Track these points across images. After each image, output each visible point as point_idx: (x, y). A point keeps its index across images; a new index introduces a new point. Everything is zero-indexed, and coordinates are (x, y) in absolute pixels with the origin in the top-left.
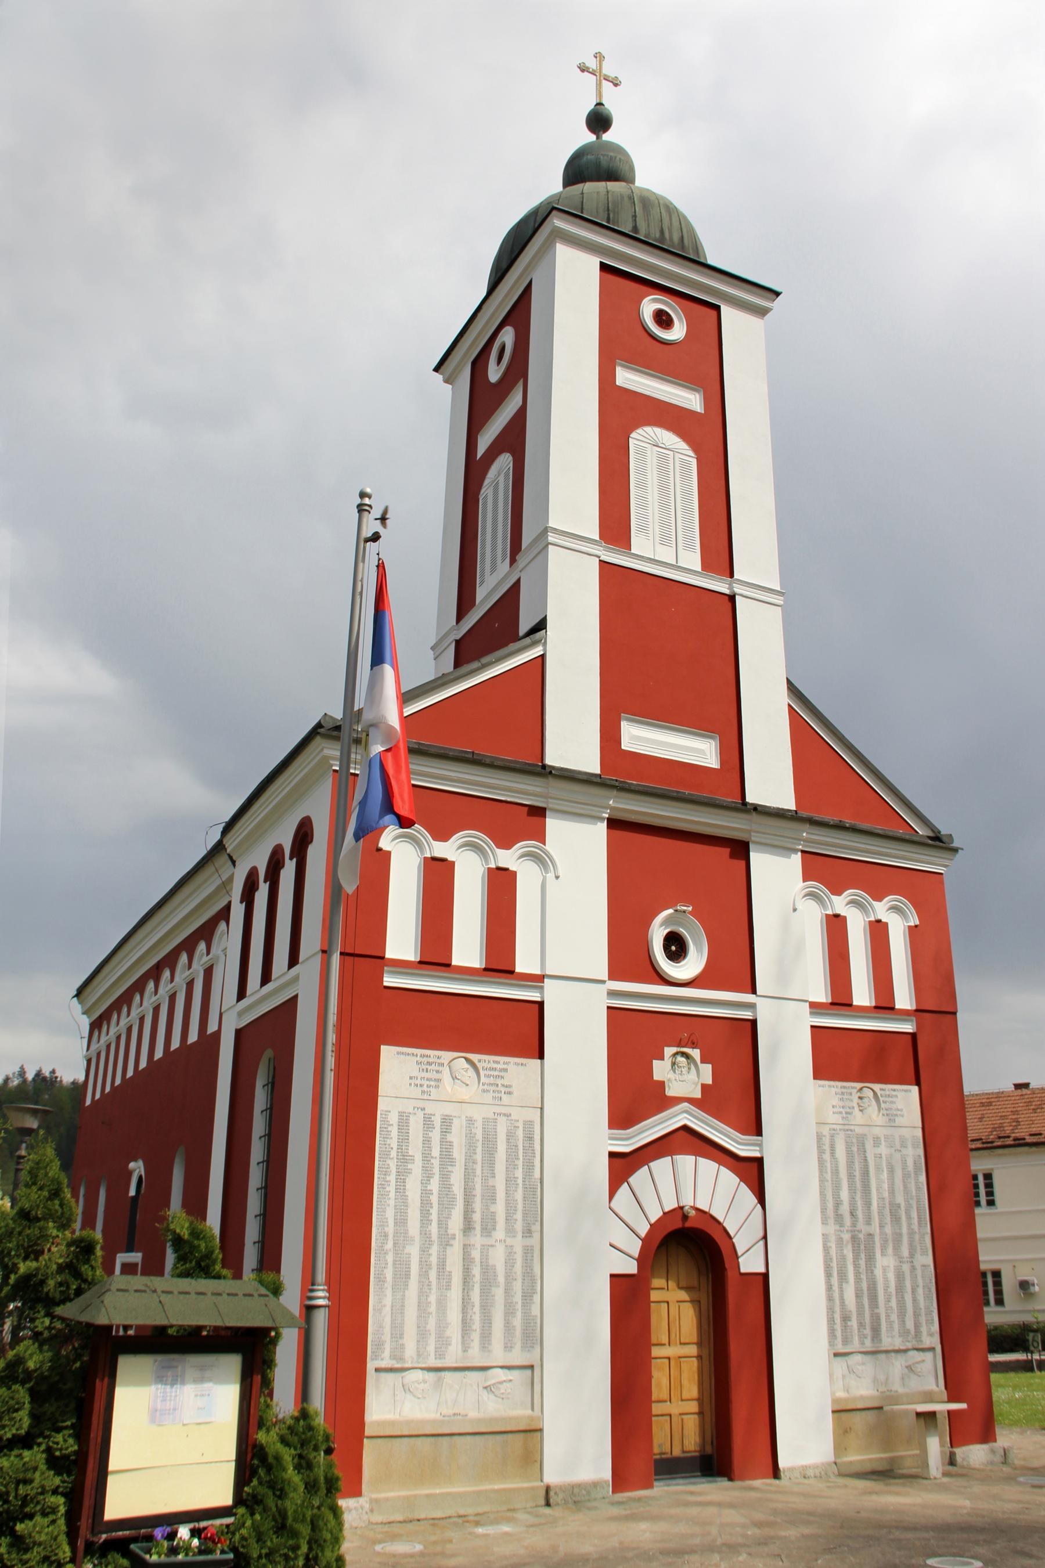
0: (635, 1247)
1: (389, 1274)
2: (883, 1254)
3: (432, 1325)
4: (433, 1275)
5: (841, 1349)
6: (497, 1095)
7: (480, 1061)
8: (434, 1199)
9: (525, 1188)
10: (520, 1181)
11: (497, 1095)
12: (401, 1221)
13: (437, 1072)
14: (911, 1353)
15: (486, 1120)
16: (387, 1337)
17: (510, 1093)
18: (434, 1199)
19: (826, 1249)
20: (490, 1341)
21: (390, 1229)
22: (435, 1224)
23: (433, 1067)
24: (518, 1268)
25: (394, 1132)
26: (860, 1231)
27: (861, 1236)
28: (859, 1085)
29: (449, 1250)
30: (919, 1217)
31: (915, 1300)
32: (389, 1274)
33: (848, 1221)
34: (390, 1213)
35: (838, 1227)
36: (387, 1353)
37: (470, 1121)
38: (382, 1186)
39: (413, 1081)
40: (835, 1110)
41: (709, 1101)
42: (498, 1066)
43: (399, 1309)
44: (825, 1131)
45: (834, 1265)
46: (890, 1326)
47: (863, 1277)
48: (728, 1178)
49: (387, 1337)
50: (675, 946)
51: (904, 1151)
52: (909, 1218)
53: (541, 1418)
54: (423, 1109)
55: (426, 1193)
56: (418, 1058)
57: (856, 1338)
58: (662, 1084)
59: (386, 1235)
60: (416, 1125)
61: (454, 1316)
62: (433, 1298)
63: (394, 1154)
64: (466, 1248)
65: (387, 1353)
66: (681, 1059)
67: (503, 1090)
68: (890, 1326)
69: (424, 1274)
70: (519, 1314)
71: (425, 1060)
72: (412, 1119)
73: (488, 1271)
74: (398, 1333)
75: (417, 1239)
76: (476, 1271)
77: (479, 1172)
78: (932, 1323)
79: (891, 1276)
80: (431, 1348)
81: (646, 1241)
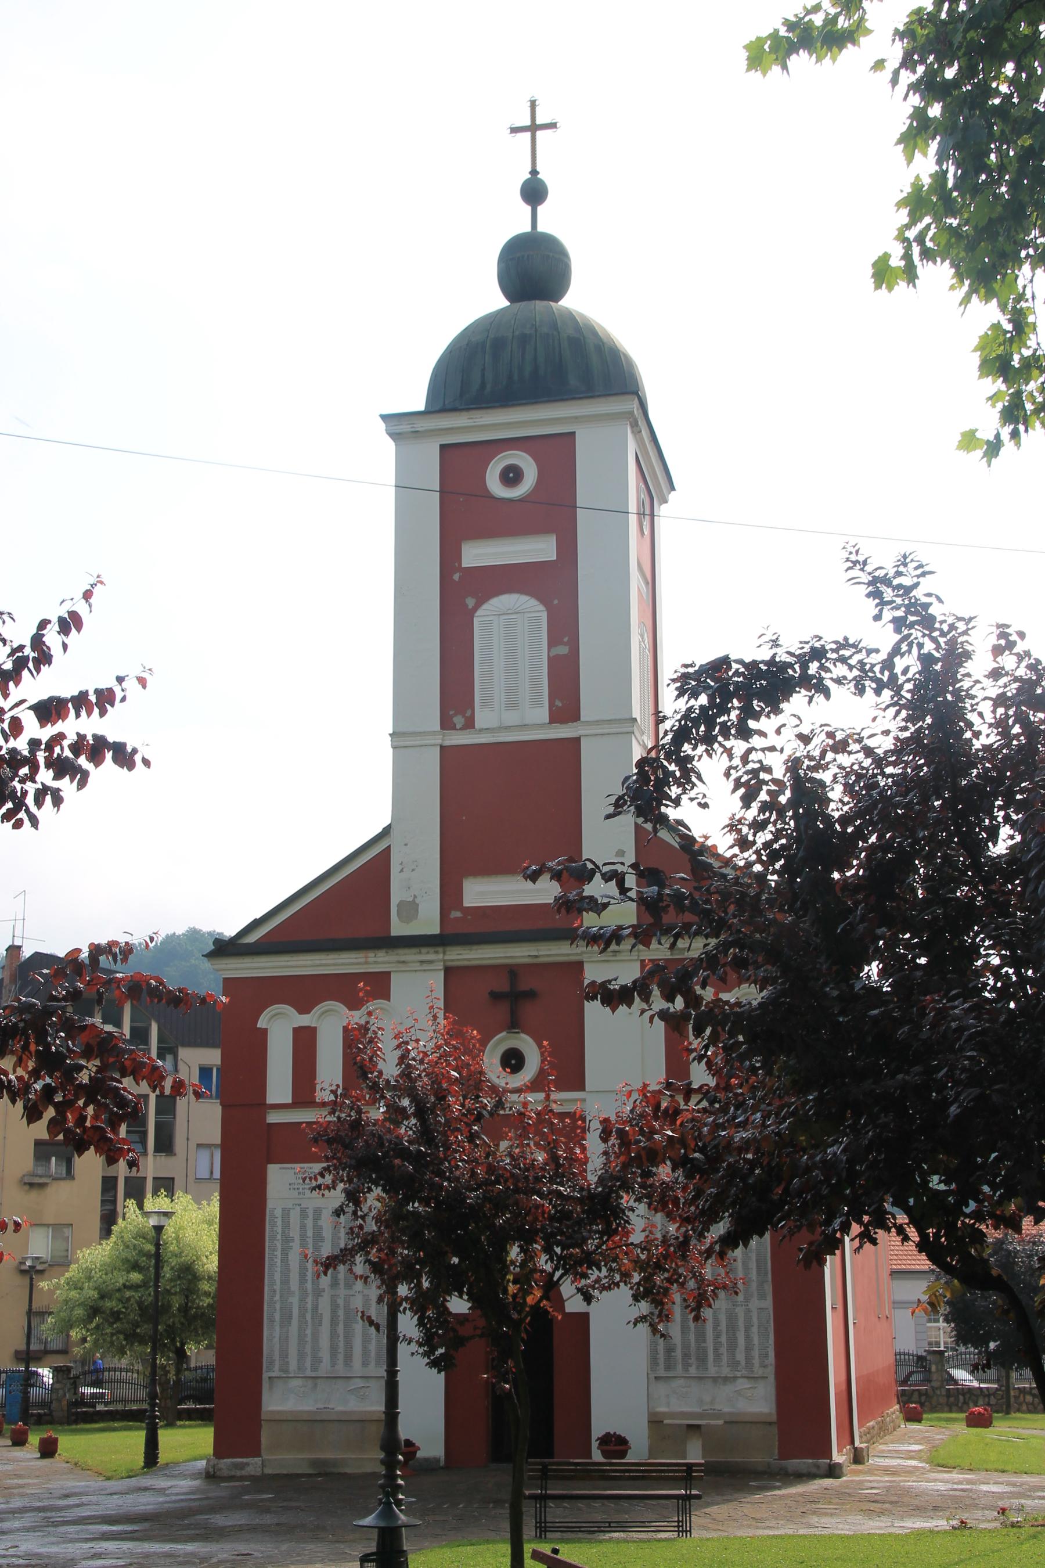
1: (277, 1316)
3: (308, 1349)
4: (309, 1316)
5: (662, 1373)
12: (285, 1281)
14: (740, 1380)
16: (276, 1357)
20: (351, 1360)
21: (277, 1287)
25: (279, 1223)
30: (758, 1267)
31: (748, 1338)
32: (277, 1316)
34: (277, 1277)
36: (277, 1367)
38: (271, 1259)
43: (285, 1340)
46: (718, 1356)
49: (276, 1357)
57: (680, 1367)
59: (275, 1291)
62: (309, 1332)
63: (279, 1237)
65: (277, 1367)
68: (718, 1356)
70: (374, 1342)
74: (284, 1355)
75: (297, 1293)
76: (341, 1313)
78: (767, 1356)
80: (308, 1364)
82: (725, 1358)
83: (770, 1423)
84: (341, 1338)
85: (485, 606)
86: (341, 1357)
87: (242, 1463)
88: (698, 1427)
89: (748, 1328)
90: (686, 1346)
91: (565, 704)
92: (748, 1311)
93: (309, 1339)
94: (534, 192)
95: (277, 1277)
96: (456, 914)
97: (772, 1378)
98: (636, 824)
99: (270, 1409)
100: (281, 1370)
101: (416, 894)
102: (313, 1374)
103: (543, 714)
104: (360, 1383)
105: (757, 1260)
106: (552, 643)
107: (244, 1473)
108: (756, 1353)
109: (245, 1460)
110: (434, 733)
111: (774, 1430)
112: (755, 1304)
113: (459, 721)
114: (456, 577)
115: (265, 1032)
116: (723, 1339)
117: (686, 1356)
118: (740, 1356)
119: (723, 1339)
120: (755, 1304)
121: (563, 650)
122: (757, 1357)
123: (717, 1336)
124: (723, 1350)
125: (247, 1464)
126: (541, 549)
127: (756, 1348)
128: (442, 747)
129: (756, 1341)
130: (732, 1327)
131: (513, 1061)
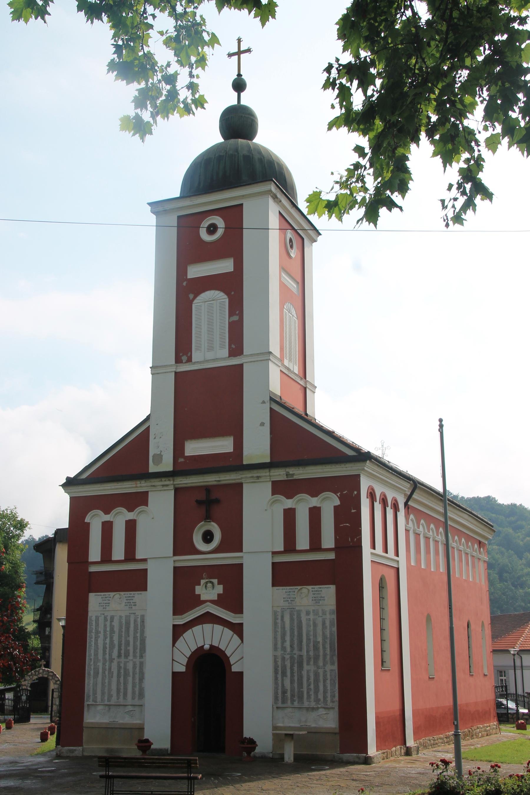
0: (185, 661)
2: (308, 664)
3: (106, 691)
4: (107, 673)
5: (280, 705)
8: (108, 646)
9: (141, 640)
10: (139, 638)
12: (96, 654)
14: (320, 710)
15: (126, 616)
16: (91, 694)
17: (135, 605)
18: (108, 646)
19: (275, 662)
21: (92, 657)
22: (108, 655)
24: (137, 670)
26: (295, 654)
27: (296, 656)
28: (299, 587)
29: (112, 663)
30: (330, 647)
31: (325, 686)
33: (288, 649)
34: (92, 652)
35: (283, 652)
37: (121, 617)
38: (90, 643)
40: (285, 600)
41: (220, 602)
43: (95, 685)
44: (279, 610)
45: (280, 669)
46: (309, 696)
47: (296, 674)
48: (228, 632)
49: (91, 694)
50: (208, 537)
51: (324, 617)
52: (324, 648)
53: (143, 724)
55: (105, 644)
57: (289, 701)
58: (199, 596)
59: (91, 659)
60: (101, 619)
61: (114, 687)
62: (107, 681)
63: (94, 631)
64: (119, 663)
66: (209, 585)
67: (133, 604)
68: (309, 696)
69: (104, 672)
70: (138, 686)
72: (100, 618)
73: (126, 670)
74: (95, 693)
75: (101, 660)
76: (122, 671)
77: (123, 635)
78: (334, 696)
79: (312, 675)
80: (106, 698)
81: (190, 659)
82: (313, 697)
83: (335, 733)
84: (122, 684)
85: (198, 298)
86: (122, 694)
87: (72, 749)
88: (291, 735)
89: (325, 681)
90: (292, 690)
91: (236, 345)
92: (325, 671)
93: (107, 684)
94: (239, 86)
95: (92, 652)
96: (181, 460)
97: (337, 709)
98: (271, 409)
99: (88, 721)
100: (93, 701)
101: (162, 451)
102: (108, 703)
103: (225, 352)
104: (130, 708)
105: (330, 644)
106: (231, 315)
107: (73, 755)
108: (329, 695)
109: (74, 748)
110: (171, 365)
111: (338, 737)
112: (329, 667)
113: (184, 358)
114: (185, 284)
115: (88, 524)
116: (312, 687)
117: (293, 696)
118: (321, 696)
119: (312, 687)
120: (329, 667)
121: (236, 318)
122: (329, 697)
123: (309, 685)
124: (312, 693)
125: (75, 750)
126: (225, 266)
127: (329, 692)
128: (176, 373)
129: (329, 688)
130: (316, 681)
131: (208, 537)
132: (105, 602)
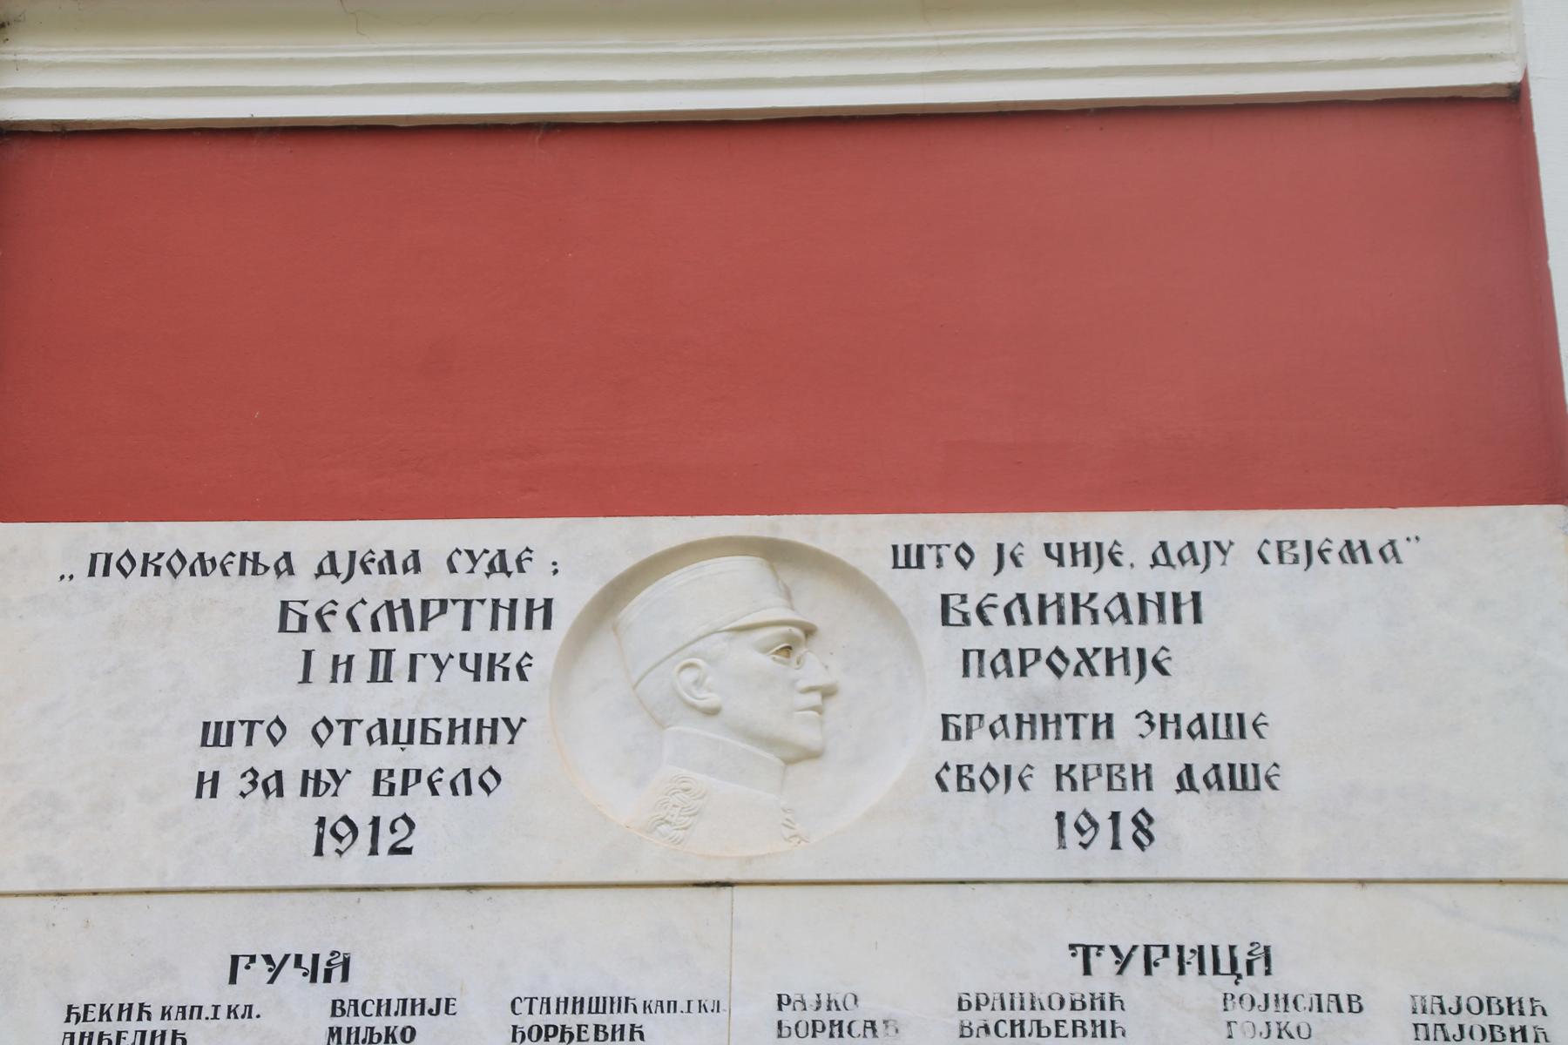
6: (1100, 802)
7: (910, 558)
11: (1100, 802)
13: (487, 668)
17: (1240, 779)
23: (445, 634)
39: (231, 762)
42: (1106, 583)
54: (328, 968)
56: (305, 588)
67: (1166, 757)
71: (375, 589)
132: (370, 702)
